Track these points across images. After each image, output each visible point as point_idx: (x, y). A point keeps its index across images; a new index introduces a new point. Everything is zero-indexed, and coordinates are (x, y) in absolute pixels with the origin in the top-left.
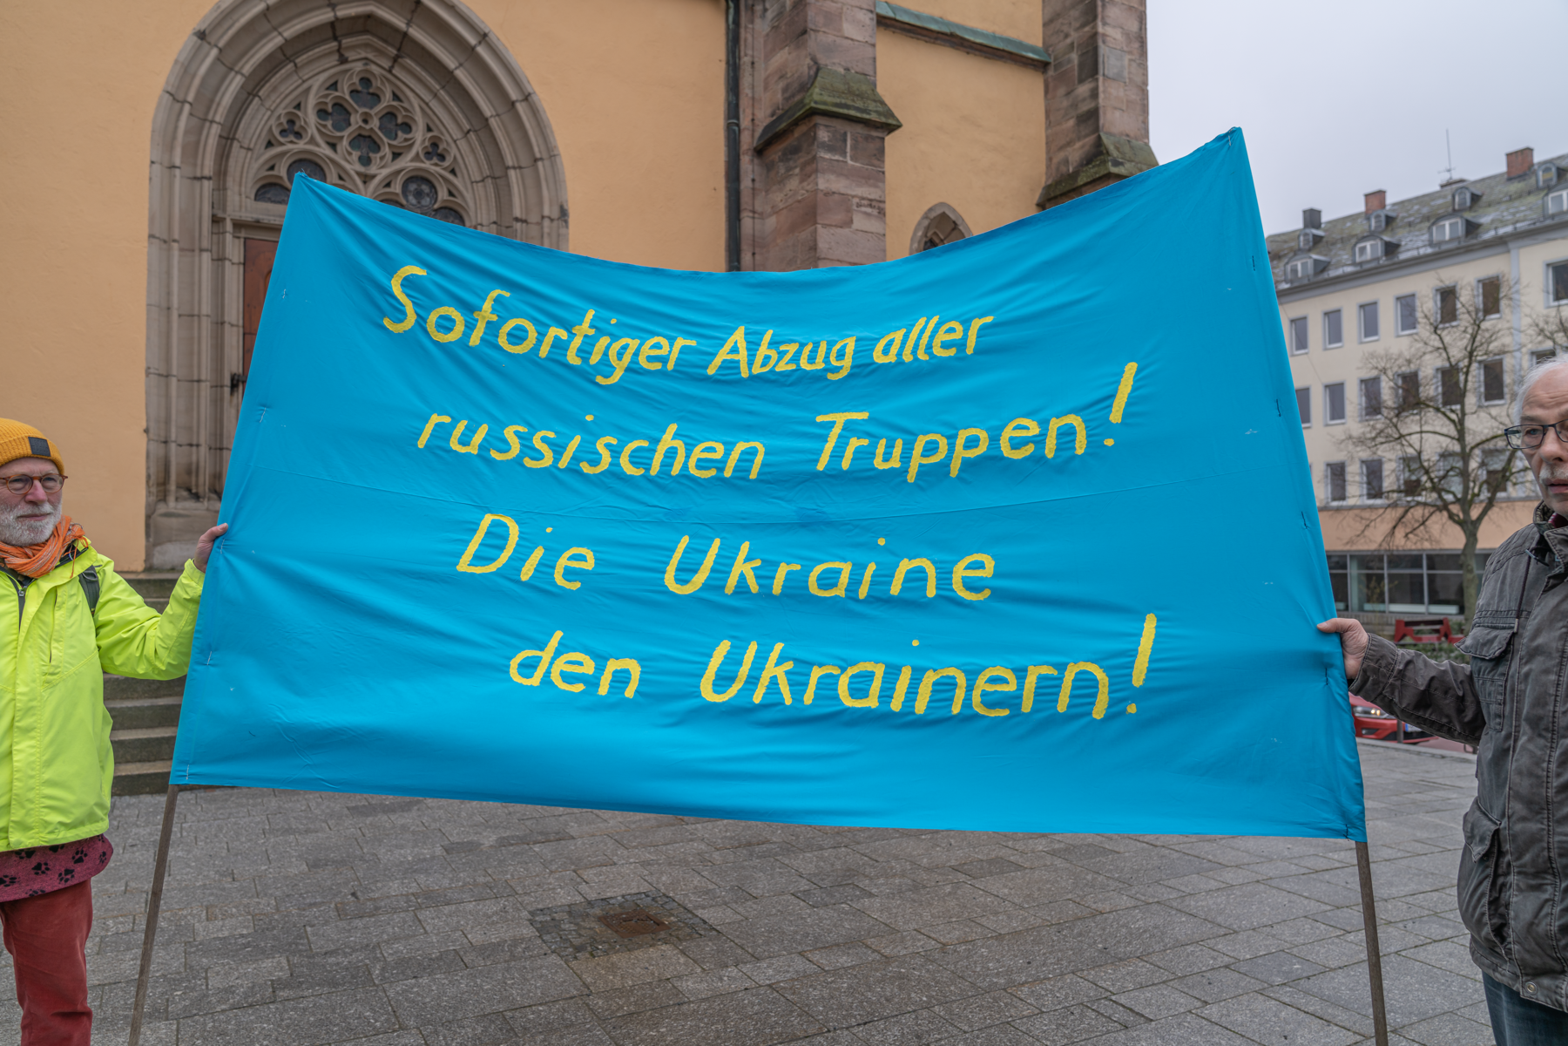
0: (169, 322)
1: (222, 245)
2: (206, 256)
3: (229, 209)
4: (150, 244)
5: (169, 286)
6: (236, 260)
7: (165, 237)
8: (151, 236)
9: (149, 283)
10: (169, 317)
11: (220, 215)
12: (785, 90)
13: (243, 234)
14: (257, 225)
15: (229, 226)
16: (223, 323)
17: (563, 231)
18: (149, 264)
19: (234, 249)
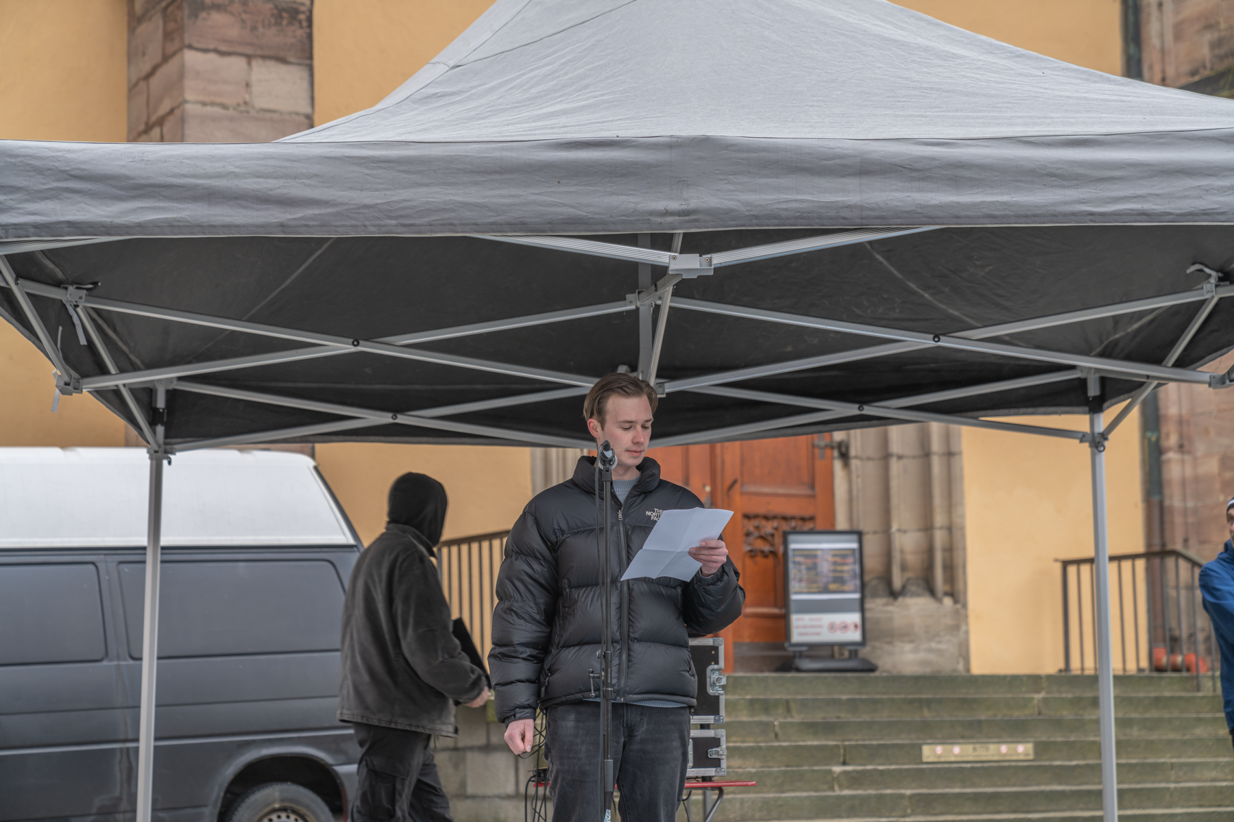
12: (1214, 45)
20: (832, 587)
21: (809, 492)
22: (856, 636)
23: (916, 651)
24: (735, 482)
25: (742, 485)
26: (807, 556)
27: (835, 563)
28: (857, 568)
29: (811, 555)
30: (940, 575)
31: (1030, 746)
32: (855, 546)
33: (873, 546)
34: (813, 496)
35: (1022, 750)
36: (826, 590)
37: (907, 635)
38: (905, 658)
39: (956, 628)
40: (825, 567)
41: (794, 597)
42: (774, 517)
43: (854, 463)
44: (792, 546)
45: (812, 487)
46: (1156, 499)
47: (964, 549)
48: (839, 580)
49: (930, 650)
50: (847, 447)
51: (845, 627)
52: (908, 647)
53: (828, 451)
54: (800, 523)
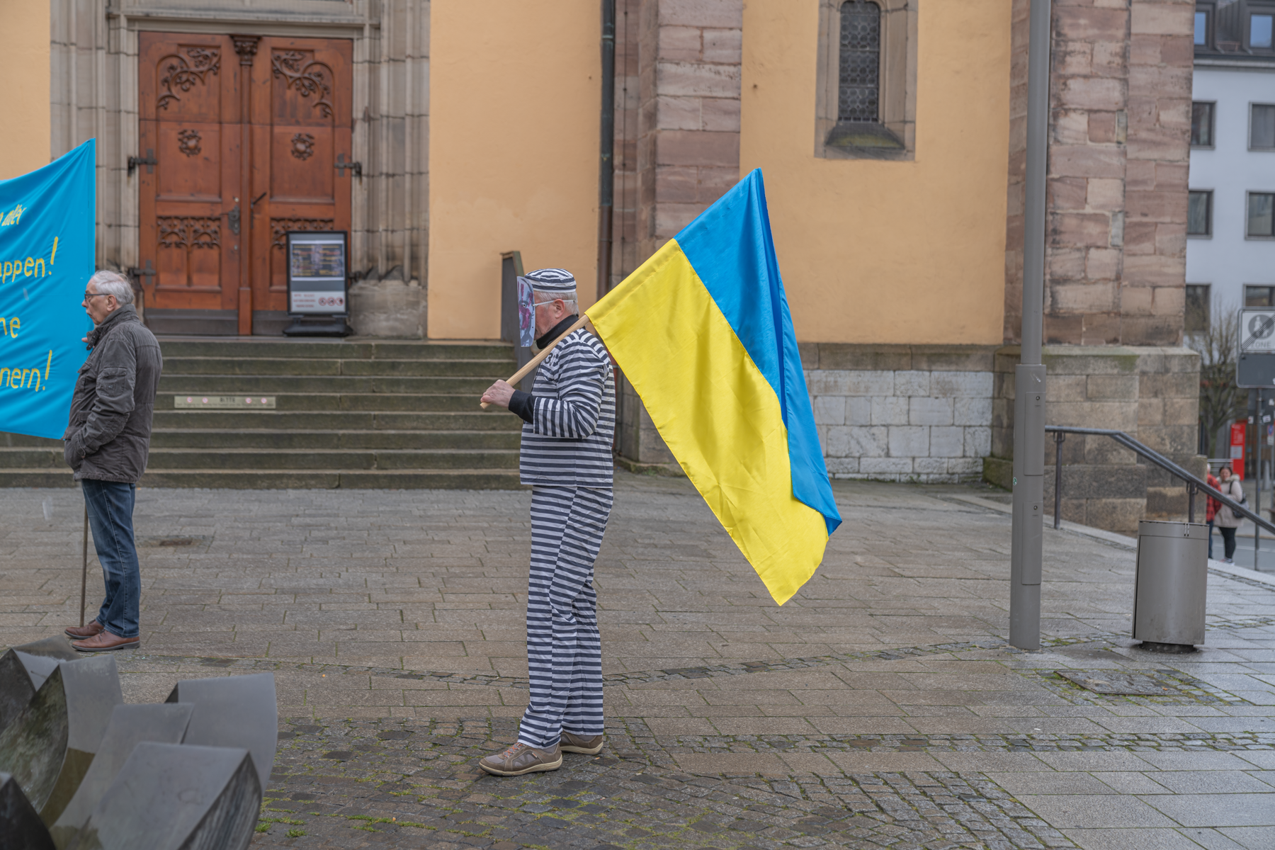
0: (69, 116)
1: (118, 38)
2: (101, 54)
3: (123, 6)
4: (52, 48)
5: (69, 84)
6: (131, 52)
7: (65, 41)
8: (53, 42)
9: (52, 84)
10: (69, 112)
11: (115, 12)
13: (137, 27)
14: (147, 19)
15: (123, 22)
16: (119, 111)
17: (425, 4)
18: (52, 67)
19: (129, 42)
20: (322, 272)
21: (330, 201)
22: (341, 308)
23: (387, 320)
24: (264, 194)
25: (271, 196)
26: (303, 250)
27: (325, 255)
28: (343, 259)
29: (306, 249)
30: (411, 265)
31: (273, 399)
32: (341, 242)
33: (357, 239)
34: (333, 204)
35: (266, 402)
36: (317, 274)
37: (382, 308)
38: (380, 325)
39: (417, 303)
40: (317, 258)
41: (293, 279)
42: (298, 220)
43: (365, 179)
44: (293, 242)
45: (333, 197)
46: (606, 205)
47: (427, 245)
48: (328, 267)
49: (396, 320)
50: (360, 168)
51: (332, 301)
52: (383, 317)
53: (348, 171)
54: (322, 224)
